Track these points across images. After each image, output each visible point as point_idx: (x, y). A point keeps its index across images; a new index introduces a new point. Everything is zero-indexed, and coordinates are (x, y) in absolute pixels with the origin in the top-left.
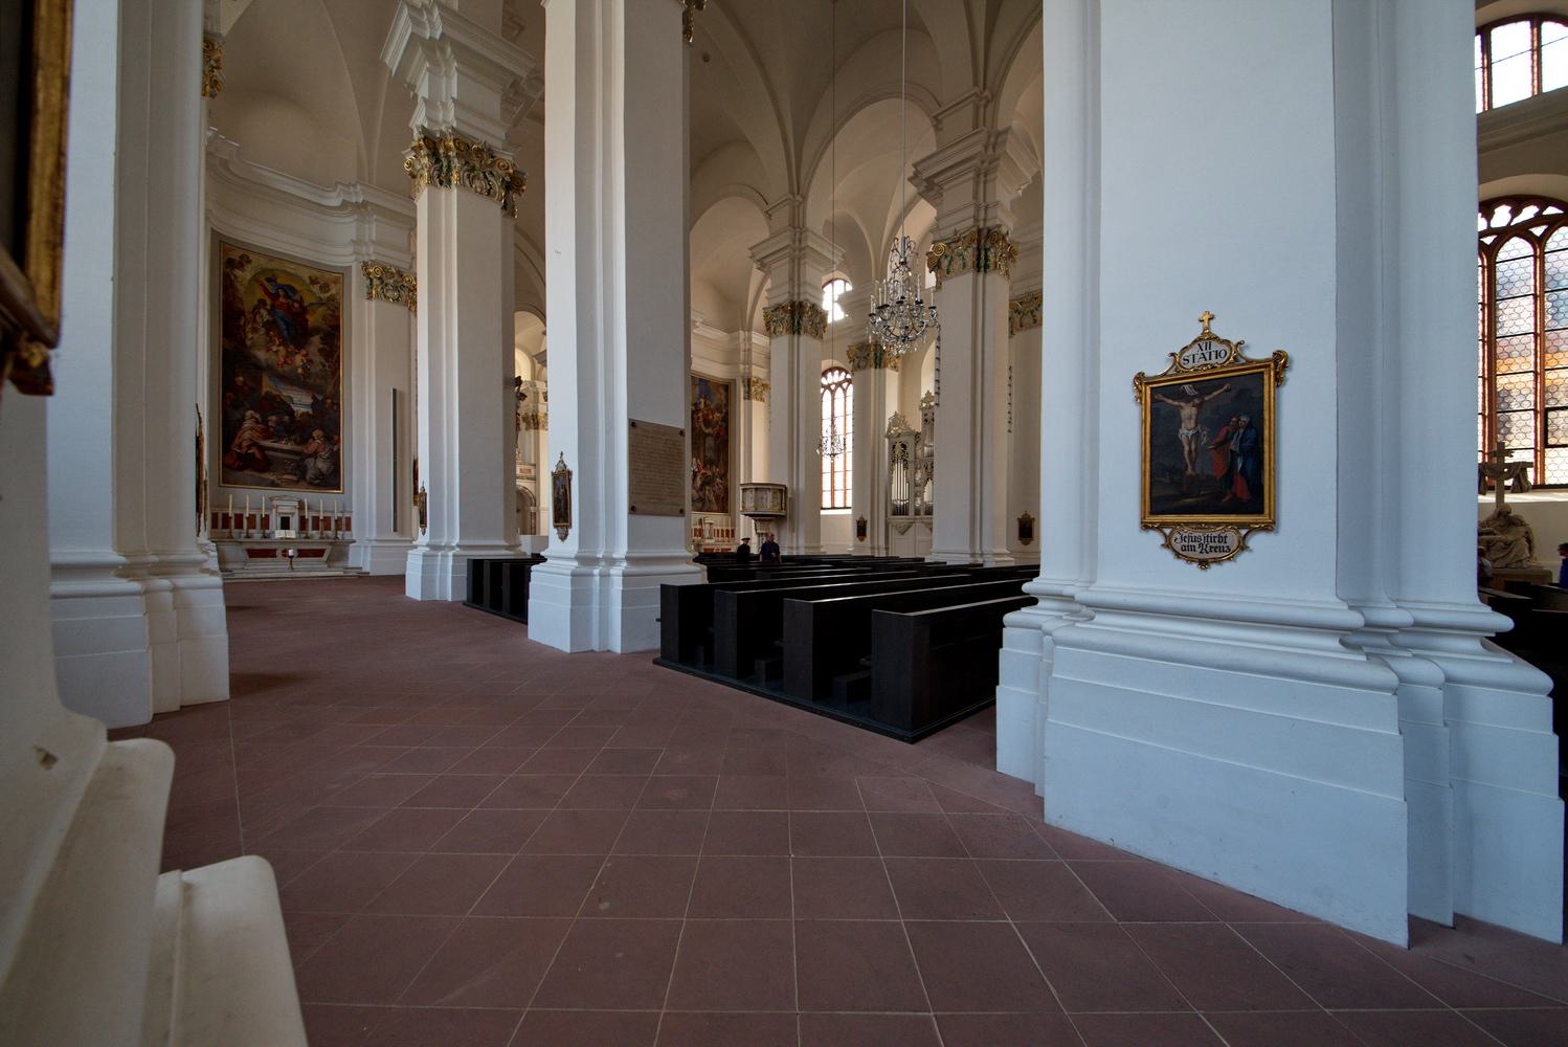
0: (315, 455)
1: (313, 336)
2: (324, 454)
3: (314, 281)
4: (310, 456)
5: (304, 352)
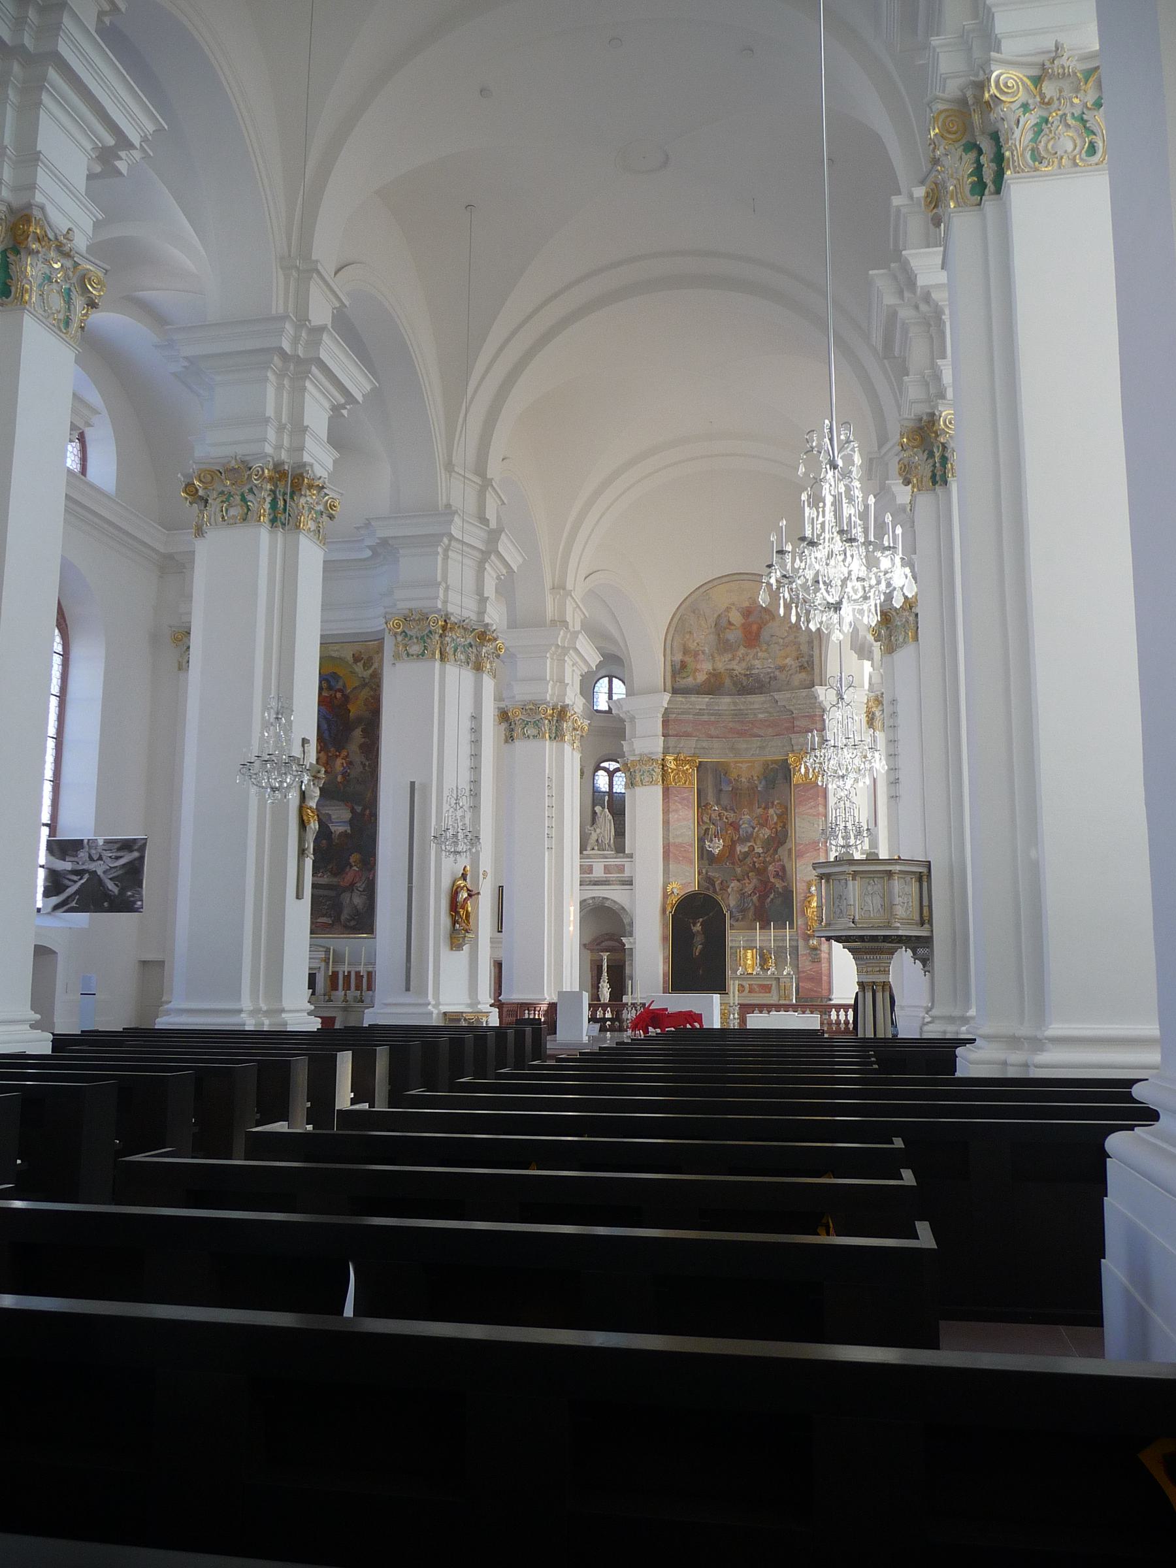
0: (351, 887)
1: (353, 730)
2: (361, 885)
3: (357, 659)
4: (345, 890)
5: (344, 753)
